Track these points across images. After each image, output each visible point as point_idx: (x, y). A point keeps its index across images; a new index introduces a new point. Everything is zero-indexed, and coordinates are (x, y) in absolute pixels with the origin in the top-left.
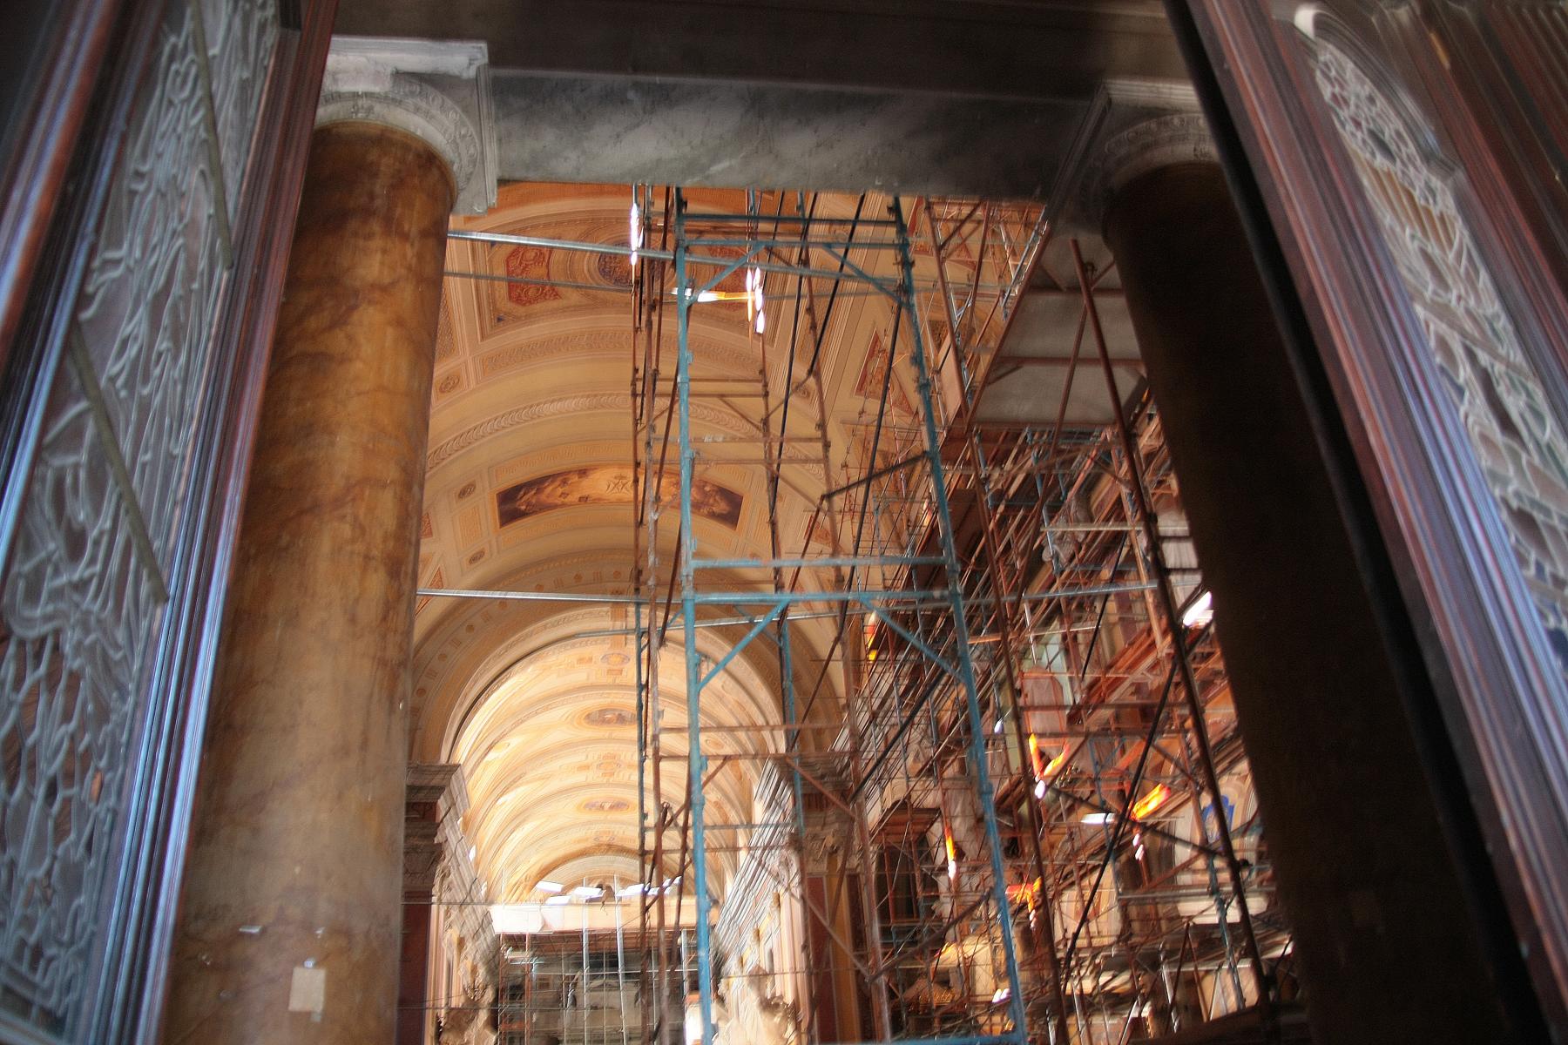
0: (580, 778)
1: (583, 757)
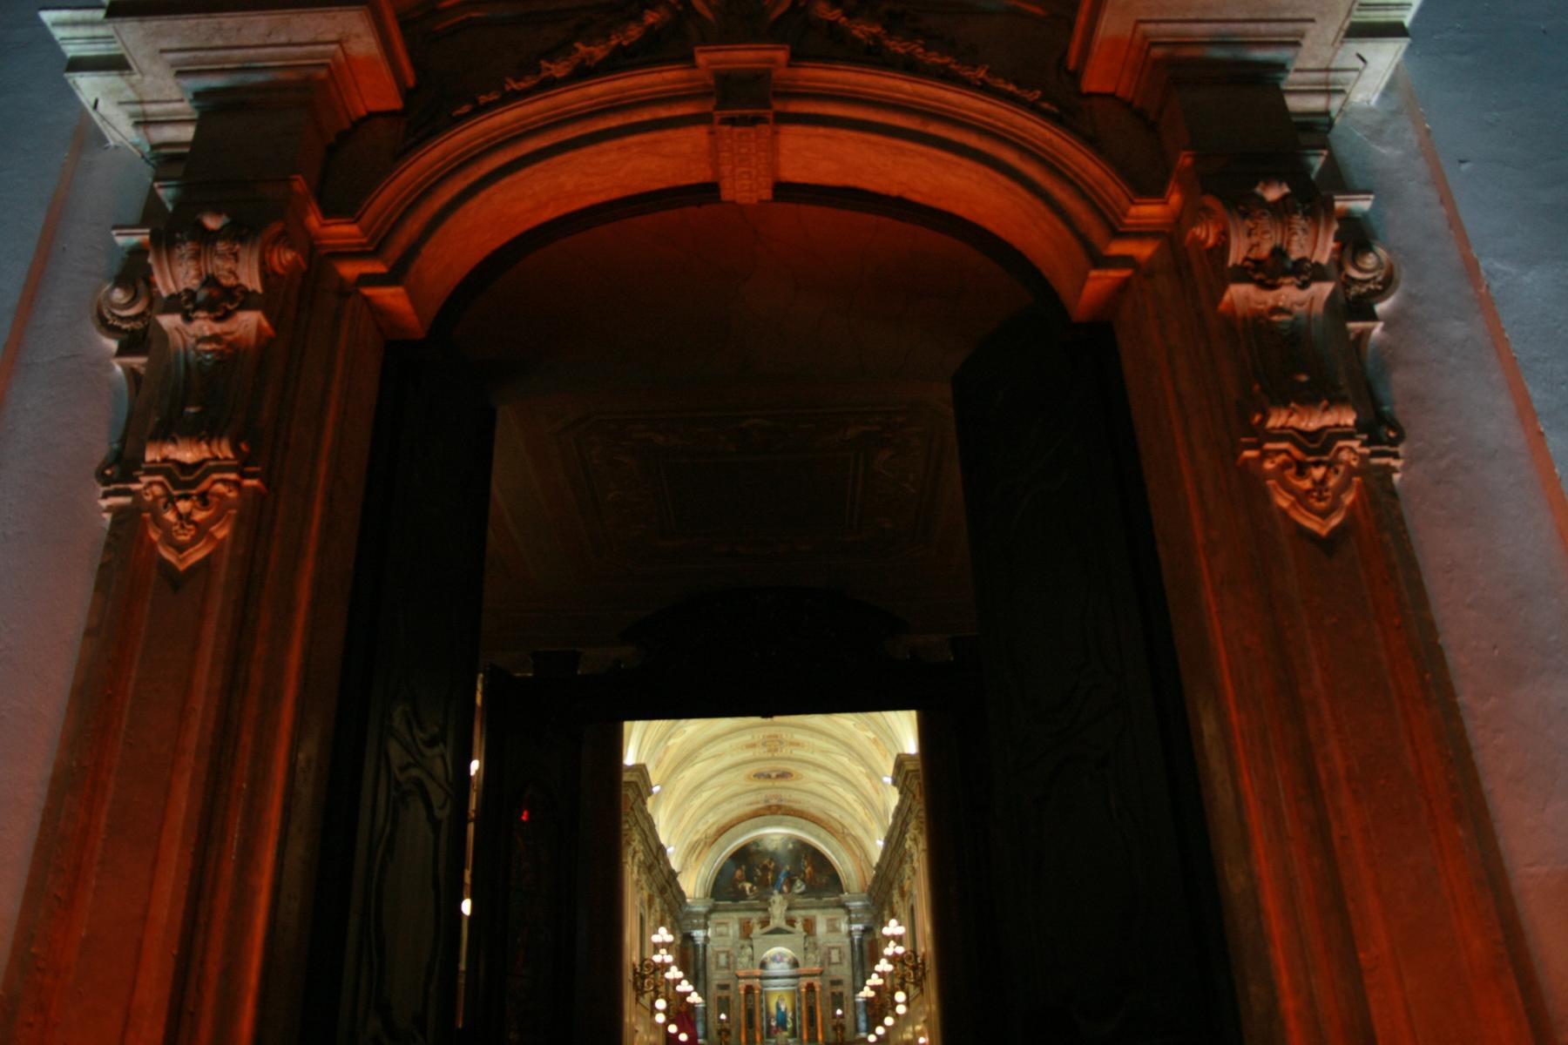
0: (749, 754)
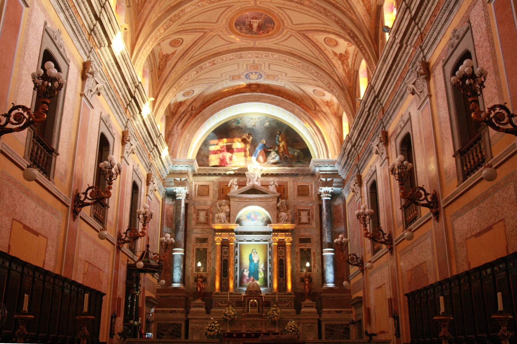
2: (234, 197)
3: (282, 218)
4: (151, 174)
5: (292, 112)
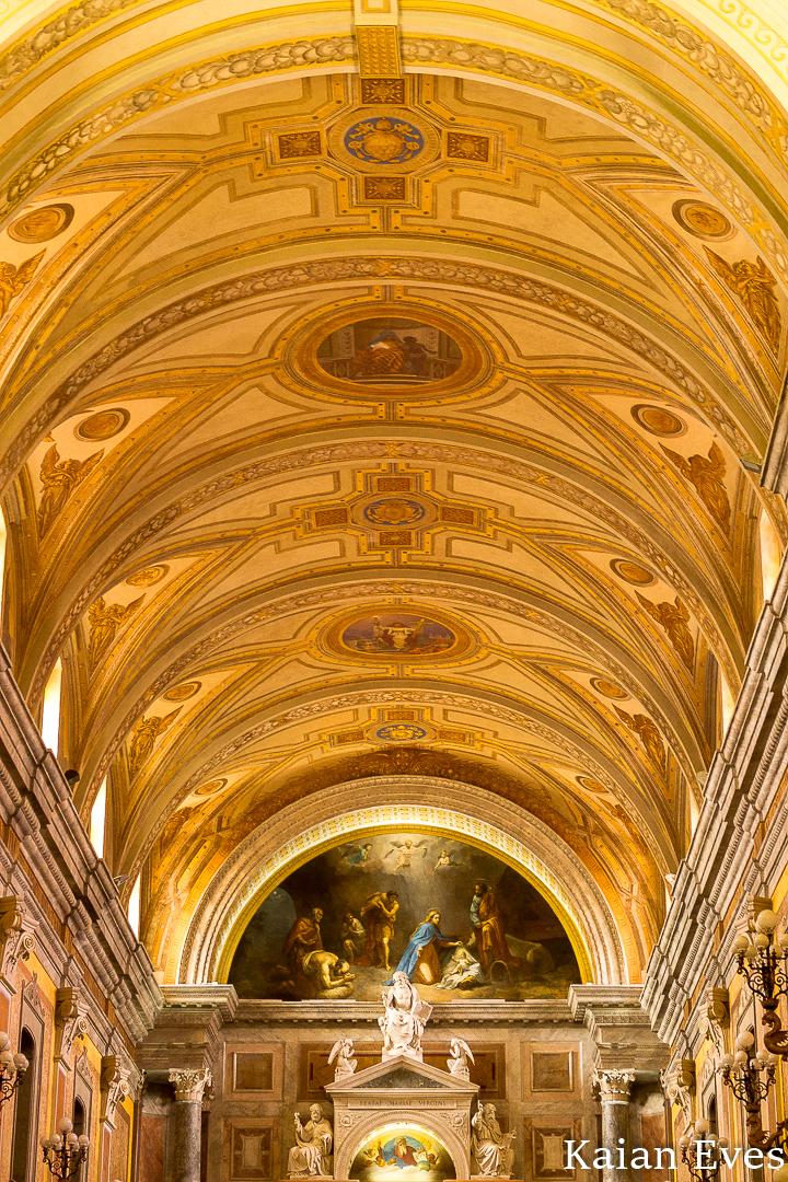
0: (322, 550)
1: (327, 484)
2: (345, 1097)
3: (485, 1160)
4: (113, 1059)
5: (517, 834)
